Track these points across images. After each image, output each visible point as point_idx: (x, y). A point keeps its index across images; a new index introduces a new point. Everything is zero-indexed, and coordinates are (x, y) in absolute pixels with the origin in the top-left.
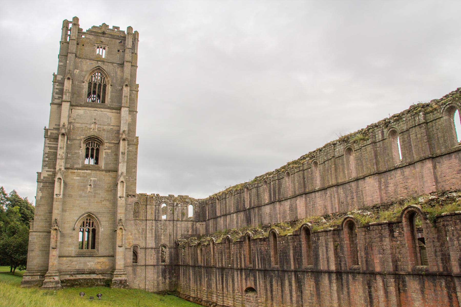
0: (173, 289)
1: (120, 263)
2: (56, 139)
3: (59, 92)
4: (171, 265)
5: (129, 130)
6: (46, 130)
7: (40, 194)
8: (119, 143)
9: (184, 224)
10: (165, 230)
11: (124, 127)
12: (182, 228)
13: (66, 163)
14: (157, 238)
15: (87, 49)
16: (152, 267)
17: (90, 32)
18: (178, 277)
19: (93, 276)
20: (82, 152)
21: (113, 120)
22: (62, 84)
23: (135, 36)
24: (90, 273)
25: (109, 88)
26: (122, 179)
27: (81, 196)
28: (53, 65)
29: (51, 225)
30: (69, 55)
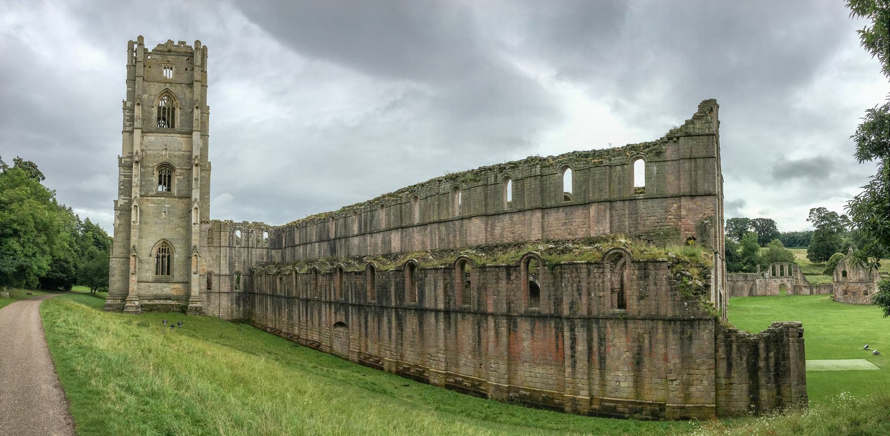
0: (247, 318)
1: (195, 290)
2: (131, 167)
3: (130, 119)
4: (245, 292)
5: (201, 155)
6: (120, 159)
7: (118, 222)
8: (191, 169)
9: (259, 251)
10: (239, 257)
11: (196, 152)
12: (258, 255)
13: (141, 190)
14: (231, 265)
15: (154, 70)
16: (226, 295)
17: (155, 51)
18: (253, 306)
19: (169, 302)
20: (156, 179)
21: (184, 145)
22: (132, 110)
23: (204, 52)
24: (166, 299)
25: (178, 112)
26: (196, 205)
27: (156, 223)
28: (121, 91)
29: (129, 252)
30: (137, 79)
